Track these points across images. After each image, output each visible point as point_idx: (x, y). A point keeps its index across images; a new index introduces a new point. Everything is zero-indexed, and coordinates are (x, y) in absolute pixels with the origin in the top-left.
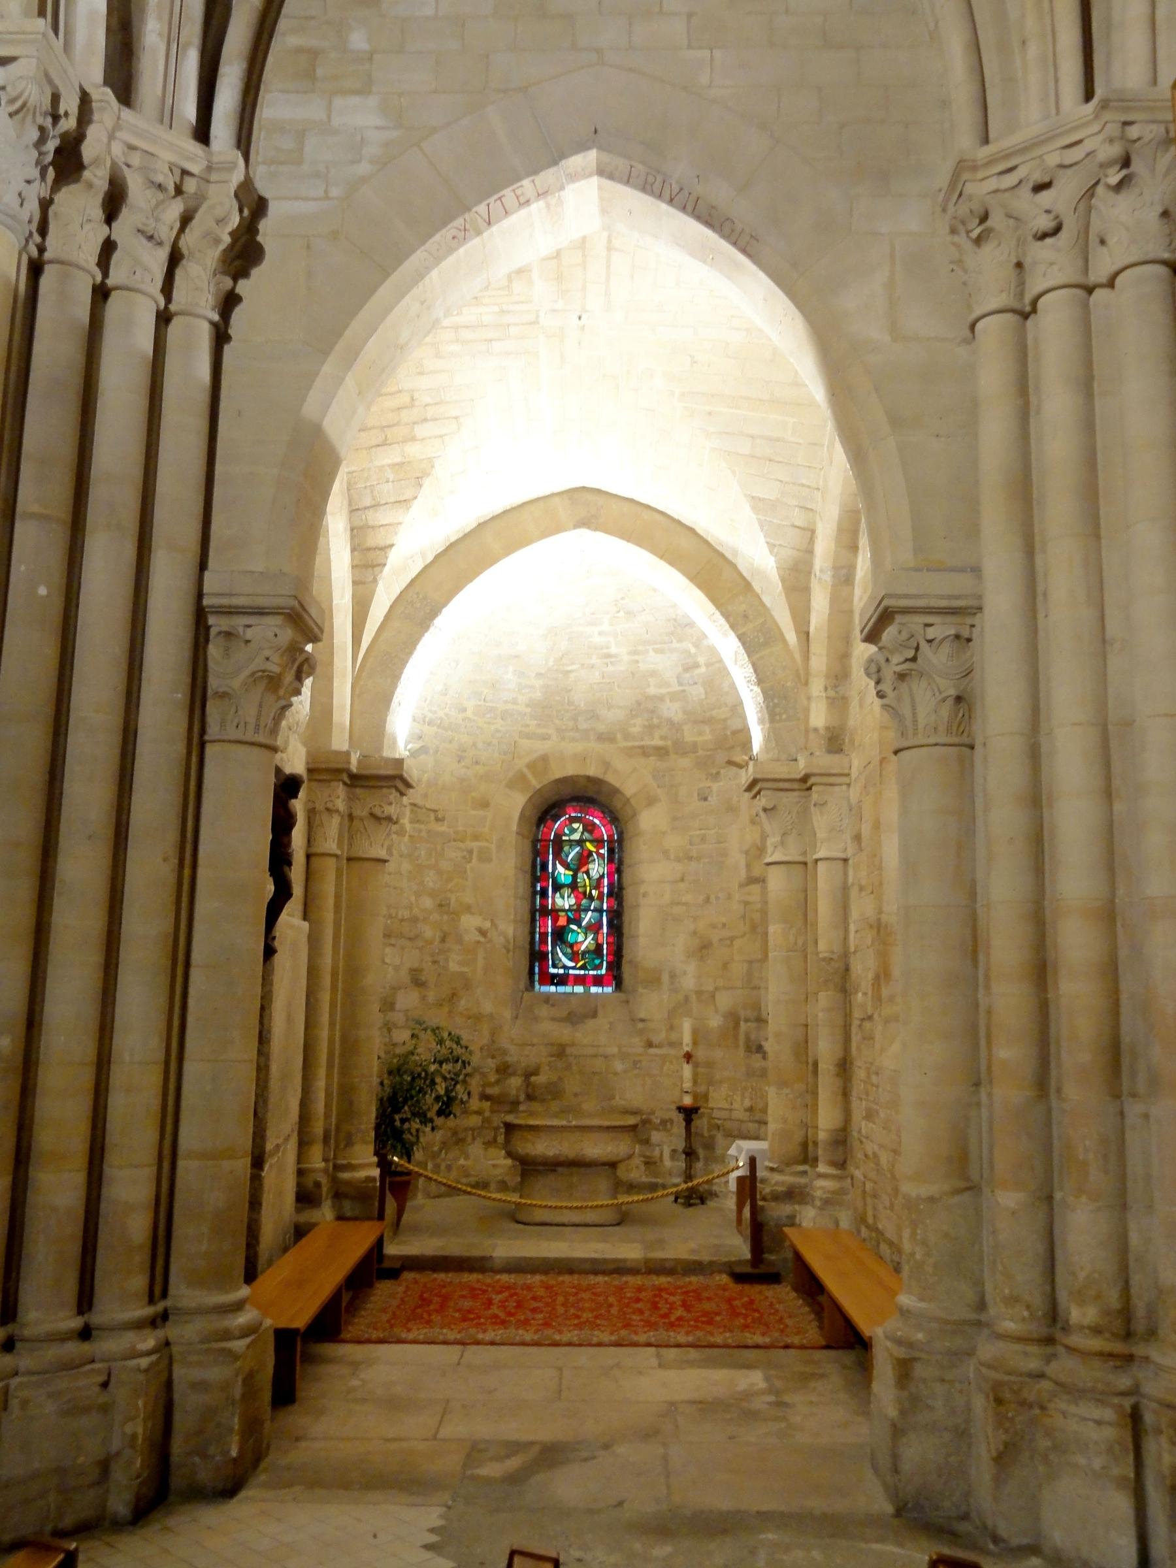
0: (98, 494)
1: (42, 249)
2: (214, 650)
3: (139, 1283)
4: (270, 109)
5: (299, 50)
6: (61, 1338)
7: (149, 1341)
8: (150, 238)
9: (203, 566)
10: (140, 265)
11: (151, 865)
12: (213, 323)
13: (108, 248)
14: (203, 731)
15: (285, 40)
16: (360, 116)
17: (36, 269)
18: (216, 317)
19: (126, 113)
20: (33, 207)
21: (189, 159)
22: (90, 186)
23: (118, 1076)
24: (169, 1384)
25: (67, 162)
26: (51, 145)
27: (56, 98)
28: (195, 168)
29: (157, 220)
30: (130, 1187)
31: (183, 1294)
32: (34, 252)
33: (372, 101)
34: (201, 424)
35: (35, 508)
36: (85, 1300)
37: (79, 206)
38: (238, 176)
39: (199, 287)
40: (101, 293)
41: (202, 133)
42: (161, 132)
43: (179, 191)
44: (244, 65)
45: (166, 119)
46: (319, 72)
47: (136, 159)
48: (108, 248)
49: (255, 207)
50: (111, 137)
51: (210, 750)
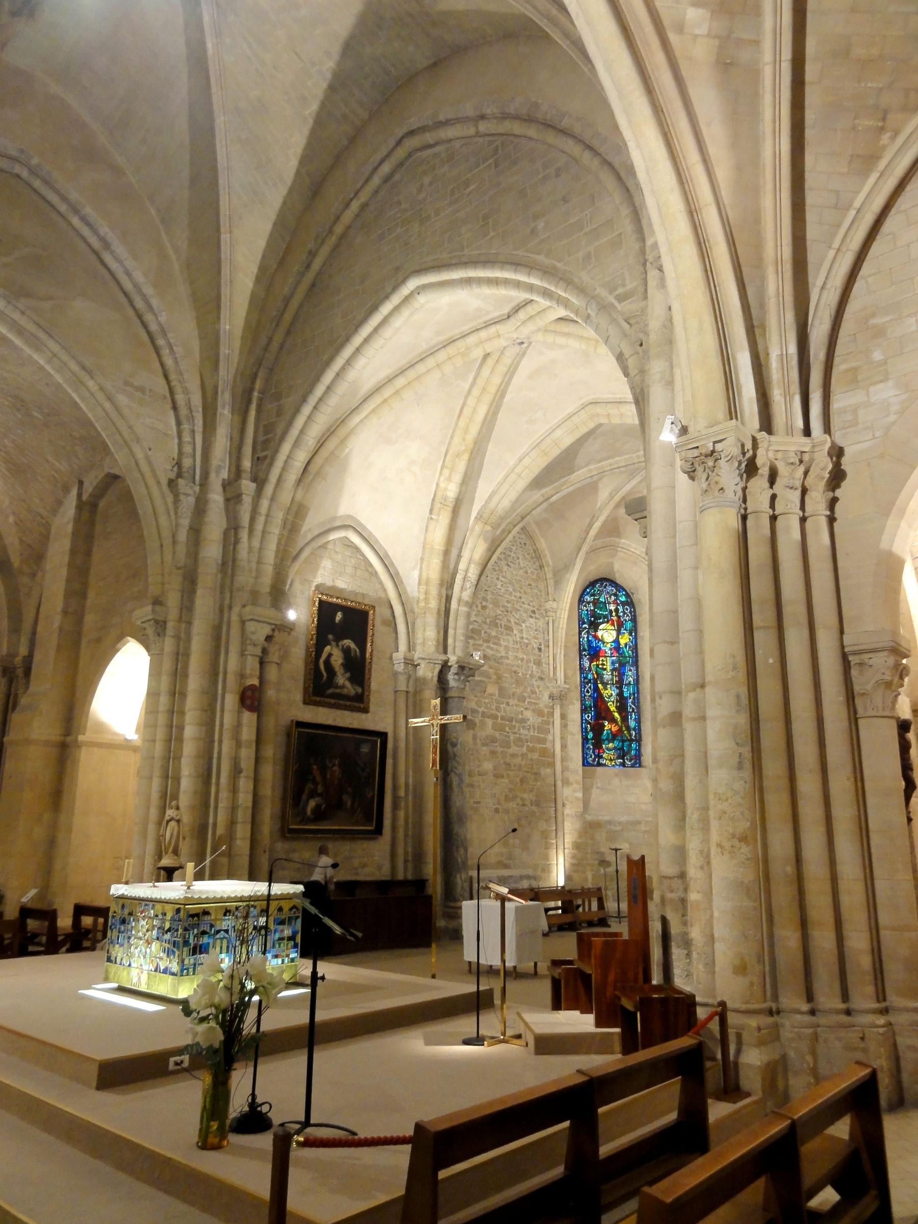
0: (787, 610)
1: (746, 509)
2: (854, 672)
3: (870, 990)
4: (837, 404)
5: (847, 371)
6: (838, 1012)
7: (881, 1021)
8: (792, 488)
9: (842, 632)
10: (789, 500)
11: (841, 783)
12: (826, 516)
13: (774, 497)
14: (855, 712)
15: (839, 367)
16: (886, 393)
17: (744, 518)
18: (828, 513)
19: (773, 438)
20: (740, 493)
21: (803, 446)
22: (762, 475)
23: (843, 885)
24: (895, 1045)
25: (751, 469)
26: (743, 465)
27: (743, 446)
28: (806, 449)
29: (793, 478)
30: (858, 941)
31: (894, 1000)
32: (743, 511)
33: (890, 383)
34: (829, 565)
35: (762, 624)
36: (845, 997)
37: (759, 484)
38: (828, 445)
39: (817, 502)
40: (774, 518)
41: (807, 432)
42: (789, 439)
43: (801, 461)
44: (821, 390)
45: (790, 431)
46: (859, 378)
47: (779, 455)
48: (774, 497)
49: (837, 453)
50: (768, 450)
51: (861, 722)
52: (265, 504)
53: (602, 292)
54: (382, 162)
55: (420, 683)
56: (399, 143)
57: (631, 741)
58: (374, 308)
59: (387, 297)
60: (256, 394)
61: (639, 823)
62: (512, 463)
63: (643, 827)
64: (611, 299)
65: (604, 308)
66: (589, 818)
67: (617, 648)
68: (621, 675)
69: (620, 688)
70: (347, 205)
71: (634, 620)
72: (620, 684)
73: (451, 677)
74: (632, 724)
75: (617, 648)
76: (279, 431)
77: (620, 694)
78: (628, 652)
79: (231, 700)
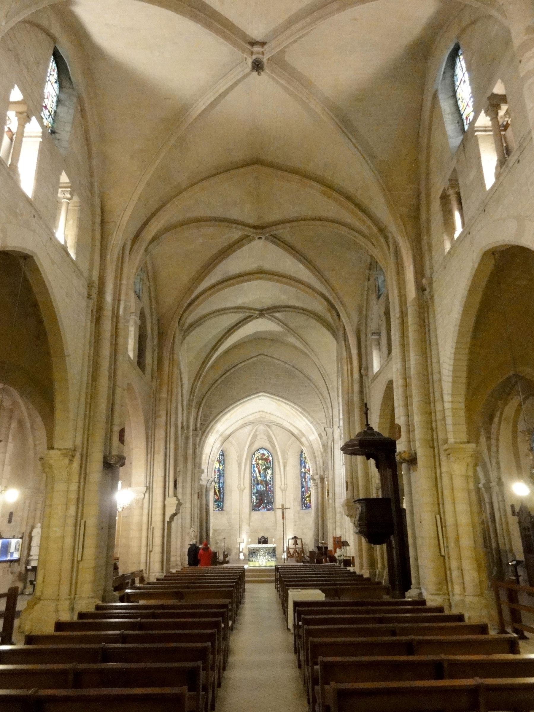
52: (204, 438)
53: (318, 420)
54: (254, 357)
55: (201, 486)
56: (261, 354)
57: (221, 502)
58: (250, 396)
59: (254, 394)
60: (203, 404)
61: (225, 530)
62: (234, 421)
63: (226, 531)
64: (319, 422)
65: (317, 423)
66: (214, 528)
67: (219, 471)
68: (219, 480)
69: (219, 484)
70: (241, 363)
71: (224, 461)
72: (219, 483)
73: (208, 484)
74: (222, 496)
75: (219, 471)
76: (211, 418)
77: (219, 486)
78: (222, 472)
79: (196, 496)
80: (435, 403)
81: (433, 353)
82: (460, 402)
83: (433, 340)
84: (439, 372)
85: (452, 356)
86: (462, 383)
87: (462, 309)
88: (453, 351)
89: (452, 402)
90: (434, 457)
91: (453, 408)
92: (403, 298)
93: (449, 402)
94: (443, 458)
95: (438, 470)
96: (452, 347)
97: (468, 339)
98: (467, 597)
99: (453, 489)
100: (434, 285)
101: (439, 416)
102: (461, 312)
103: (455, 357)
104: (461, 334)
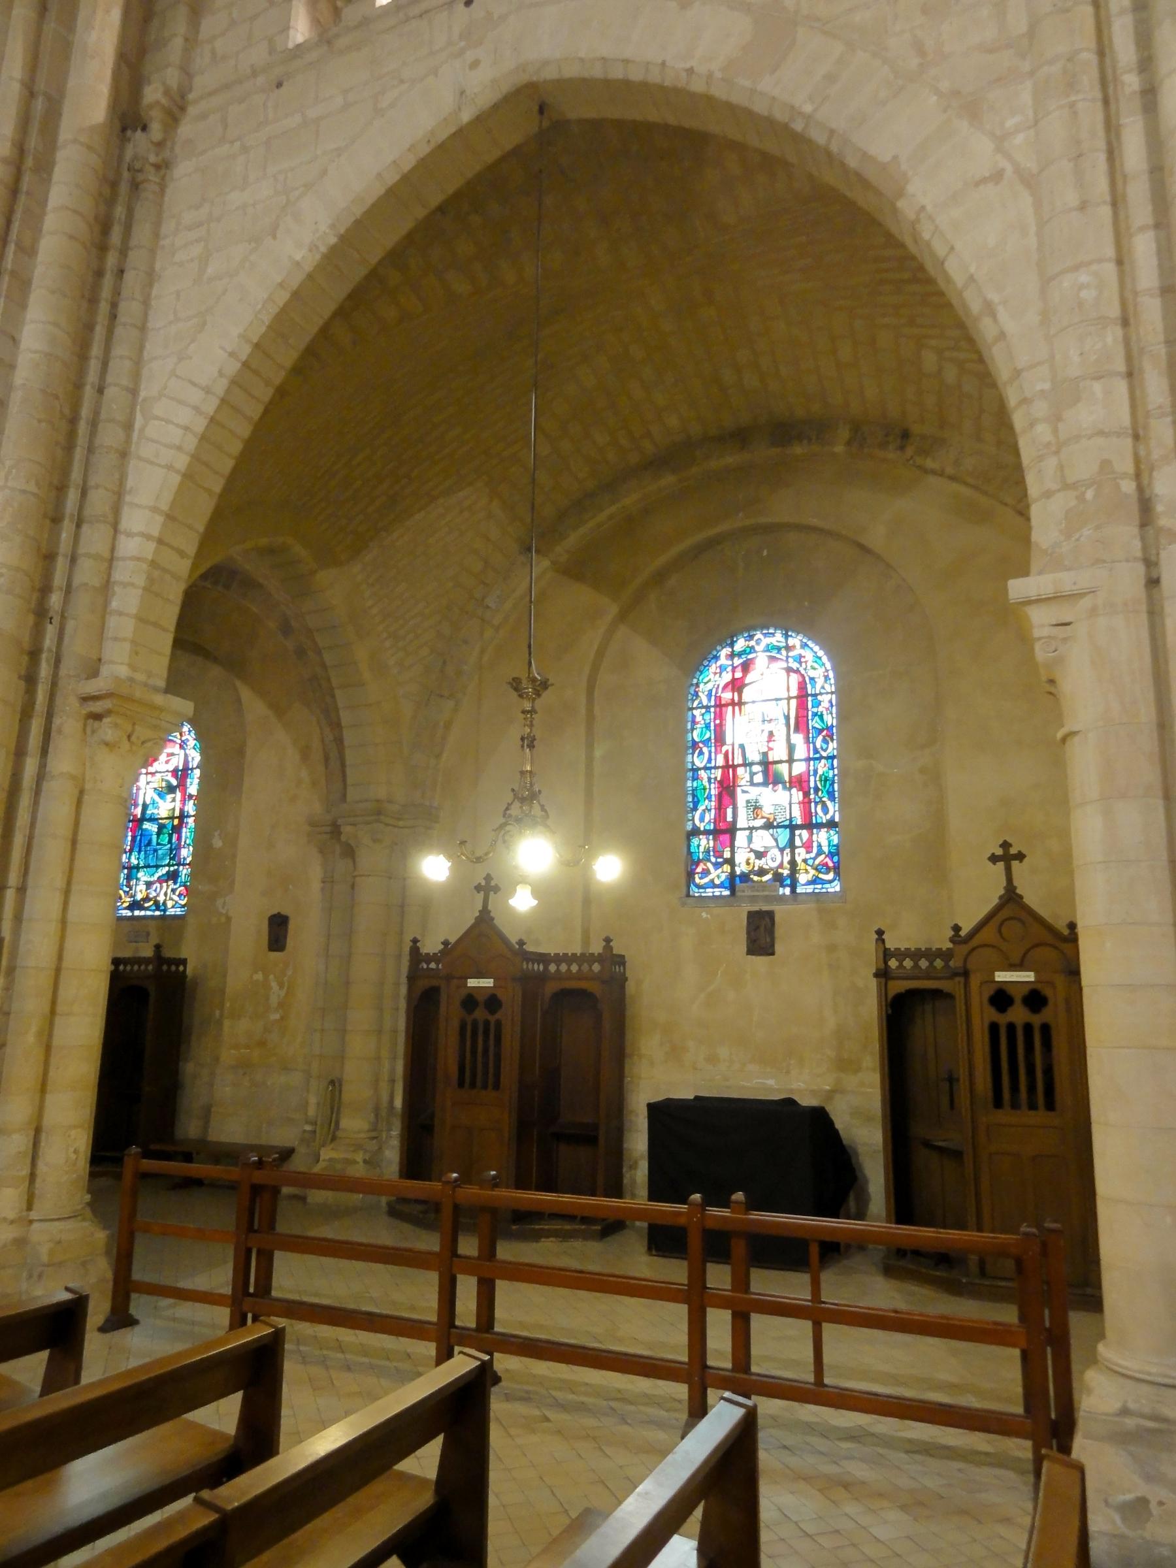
80: (79, 526)
81: (120, 350)
82: (182, 554)
83: (129, 309)
84: (128, 426)
85: (221, 387)
86: (209, 491)
87: (333, 240)
88: (233, 367)
89: (160, 541)
90: (26, 714)
91: (153, 564)
92: (39, 105)
93: (148, 537)
94: (68, 723)
95: (31, 766)
96: (232, 354)
97: (288, 357)
98: (35, 1226)
99: (74, 842)
100: (186, 129)
101: (87, 573)
102: (323, 249)
103: (228, 391)
104: (280, 325)
